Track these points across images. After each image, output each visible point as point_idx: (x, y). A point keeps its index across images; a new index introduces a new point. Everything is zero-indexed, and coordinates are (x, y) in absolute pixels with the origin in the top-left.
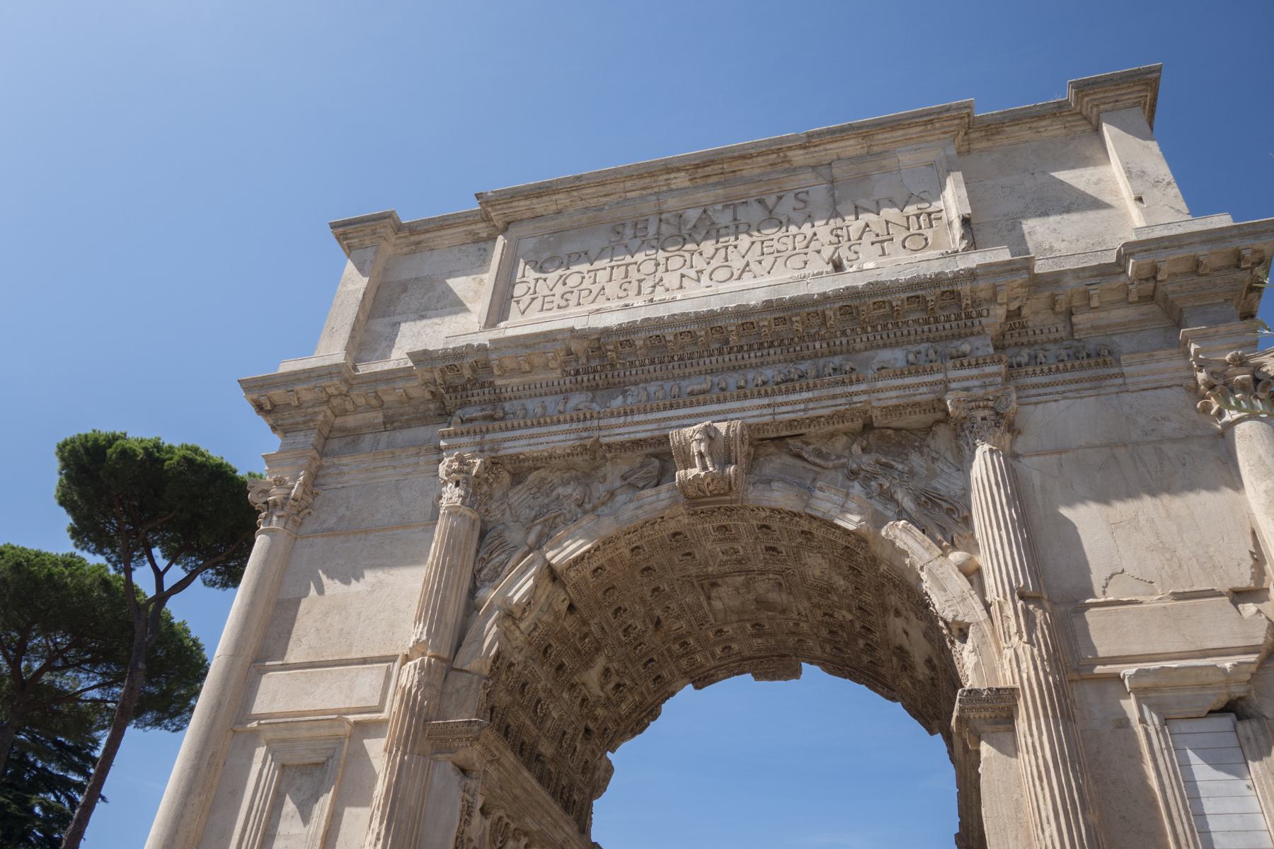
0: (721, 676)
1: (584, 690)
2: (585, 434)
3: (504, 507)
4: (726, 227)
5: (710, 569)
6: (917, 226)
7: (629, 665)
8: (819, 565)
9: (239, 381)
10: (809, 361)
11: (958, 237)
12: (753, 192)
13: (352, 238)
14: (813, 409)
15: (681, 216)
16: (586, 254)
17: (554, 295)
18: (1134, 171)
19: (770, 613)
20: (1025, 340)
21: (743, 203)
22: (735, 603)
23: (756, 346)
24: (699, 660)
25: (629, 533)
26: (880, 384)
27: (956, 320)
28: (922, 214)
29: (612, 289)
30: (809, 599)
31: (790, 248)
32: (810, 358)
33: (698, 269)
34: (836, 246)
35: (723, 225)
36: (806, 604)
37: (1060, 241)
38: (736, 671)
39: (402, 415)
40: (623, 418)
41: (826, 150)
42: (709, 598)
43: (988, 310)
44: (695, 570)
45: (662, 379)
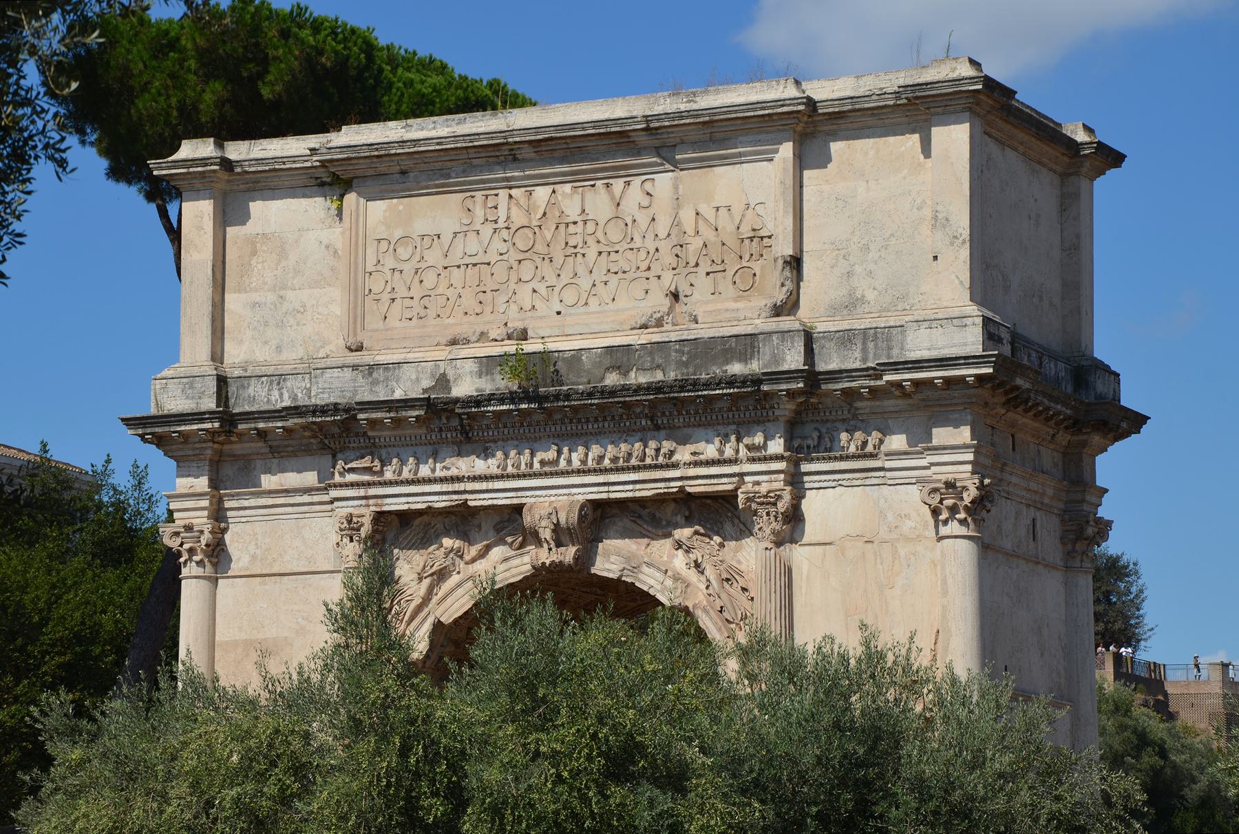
2: (455, 497)
4: (575, 223)
6: (747, 257)
9: (123, 420)
10: (639, 434)
11: (779, 284)
12: (599, 175)
13: (180, 179)
14: (640, 490)
15: (531, 194)
16: (439, 237)
17: (412, 298)
18: (940, 216)
20: (819, 418)
21: (593, 186)
23: (592, 420)
26: (692, 472)
28: (754, 237)
29: (469, 301)
31: (633, 270)
32: (639, 430)
33: (548, 284)
34: (675, 272)
35: (571, 219)
37: (871, 290)
39: (287, 446)
40: (485, 483)
41: (668, 133)
43: (778, 403)
45: (517, 439)
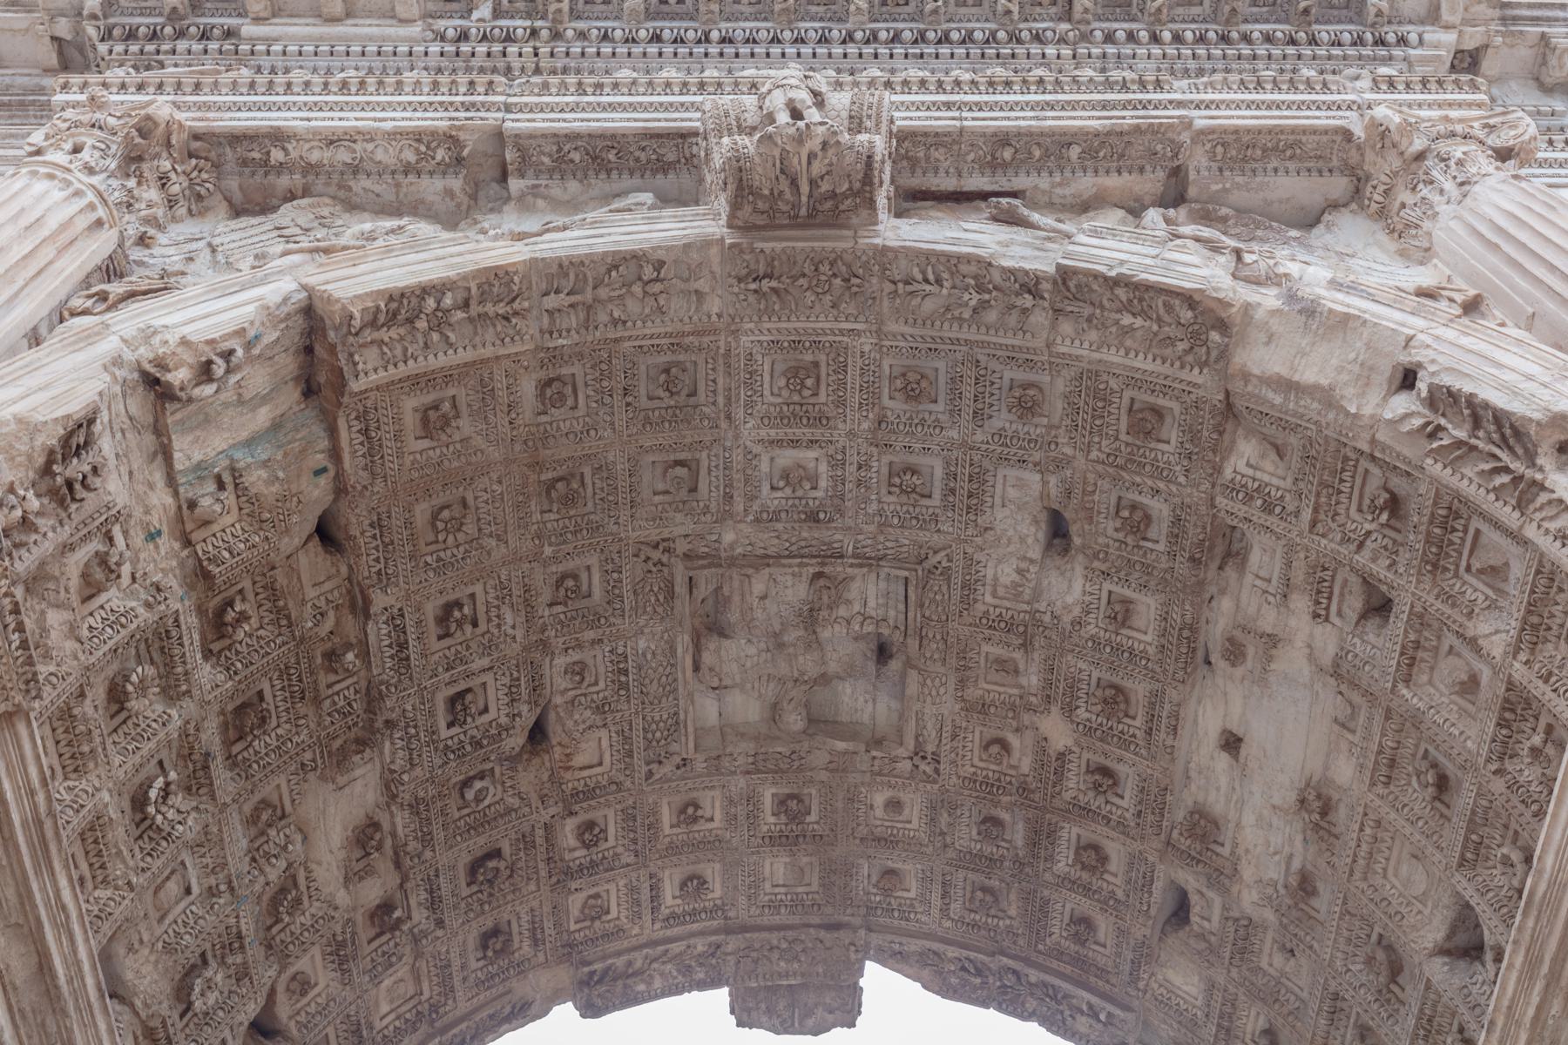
0: (658, 983)
1: (296, 848)
3: (194, 246)
5: (729, 537)
7: (439, 835)
8: (1022, 540)
19: (841, 745)
22: (746, 708)
24: (614, 913)
25: (557, 292)
27: (1355, 44)
30: (962, 683)
36: (950, 707)
38: (701, 975)
42: (696, 668)
44: (689, 527)
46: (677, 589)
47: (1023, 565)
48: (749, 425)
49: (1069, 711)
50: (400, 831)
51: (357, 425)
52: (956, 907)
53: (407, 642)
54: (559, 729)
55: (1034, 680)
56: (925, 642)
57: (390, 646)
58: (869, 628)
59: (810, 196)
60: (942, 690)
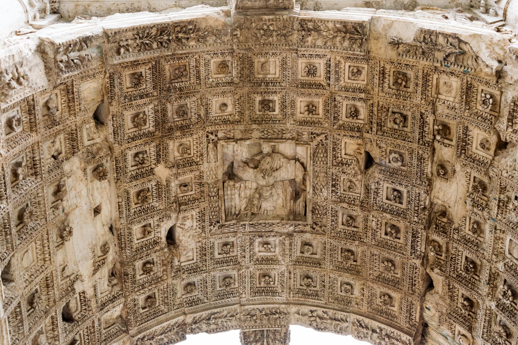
8: (184, 236)
30: (201, 177)
46: (311, 214)
47: (182, 226)
48: (283, 269)
49: (158, 184)
50: (430, 164)
51: (413, 317)
52: (193, 64)
53: (412, 243)
54: (360, 163)
55: (173, 184)
56: (217, 193)
57: (418, 242)
58: (237, 185)
59: (263, 341)
60: (208, 173)
